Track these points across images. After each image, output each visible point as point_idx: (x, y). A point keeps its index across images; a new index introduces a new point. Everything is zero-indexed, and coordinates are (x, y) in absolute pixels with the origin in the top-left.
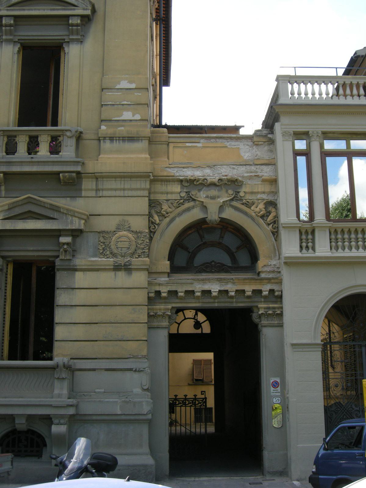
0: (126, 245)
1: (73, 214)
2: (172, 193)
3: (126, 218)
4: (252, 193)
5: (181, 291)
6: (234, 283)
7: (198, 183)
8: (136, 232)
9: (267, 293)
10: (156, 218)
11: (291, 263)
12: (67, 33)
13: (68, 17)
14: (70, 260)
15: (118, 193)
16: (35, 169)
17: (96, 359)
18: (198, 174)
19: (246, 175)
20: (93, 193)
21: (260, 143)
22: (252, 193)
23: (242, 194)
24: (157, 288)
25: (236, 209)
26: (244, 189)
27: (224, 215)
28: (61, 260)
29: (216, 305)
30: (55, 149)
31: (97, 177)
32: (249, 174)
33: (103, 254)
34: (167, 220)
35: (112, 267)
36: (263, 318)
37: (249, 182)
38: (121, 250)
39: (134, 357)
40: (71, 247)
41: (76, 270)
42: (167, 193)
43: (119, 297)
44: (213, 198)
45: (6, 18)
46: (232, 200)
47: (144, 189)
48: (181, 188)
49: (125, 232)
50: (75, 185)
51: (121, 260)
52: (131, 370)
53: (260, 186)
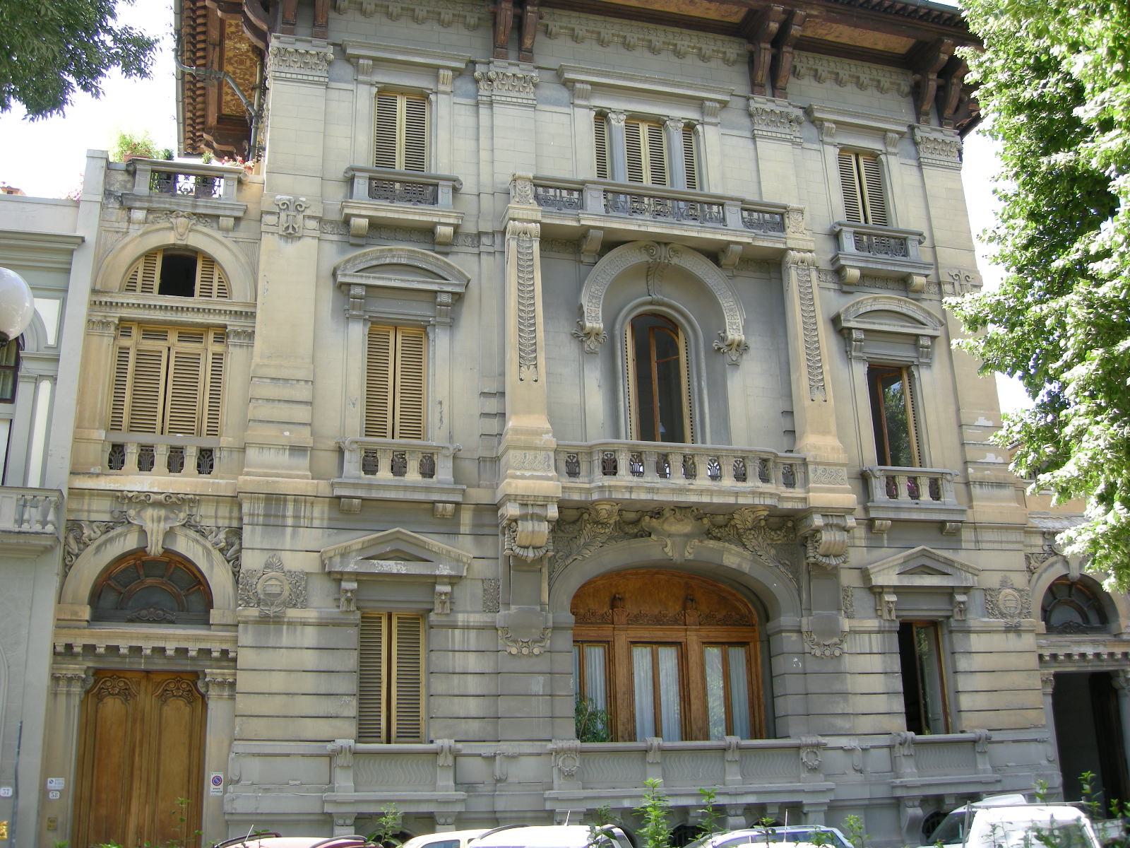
2: (1035, 546)
3: (1008, 574)
5: (1061, 652)
6: (1105, 645)
12: (914, 355)
13: (917, 336)
16: (923, 516)
20: (972, 546)
31: (975, 527)
33: (994, 616)
34: (1036, 576)
35: (1004, 629)
39: (1036, 727)
41: (969, 632)
42: (1031, 546)
43: (1013, 661)
45: (857, 331)
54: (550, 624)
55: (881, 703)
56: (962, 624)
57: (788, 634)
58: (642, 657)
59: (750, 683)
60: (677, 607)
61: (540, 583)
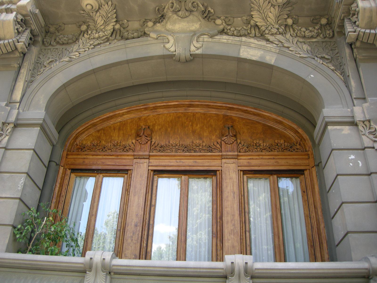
54: (12, 119)
57: (338, 127)
59: (308, 217)
60: (214, 137)
61: (16, 80)
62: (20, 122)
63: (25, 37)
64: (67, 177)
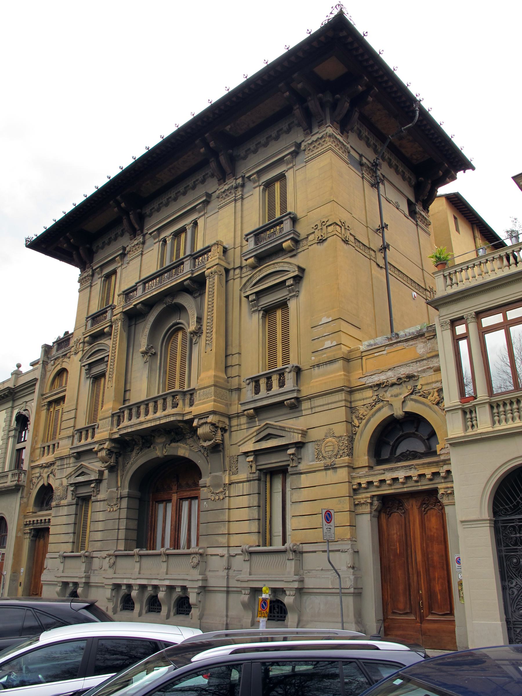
0: (331, 448)
1: (291, 430)
4: (428, 384)
5: (375, 479)
7: (384, 386)
8: (339, 437)
9: (444, 474)
10: (356, 422)
11: (456, 444)
13: (284, 282)
14: (296, 466)
15: (326, 407)
17: (317, 543)
18: (382, 378)
19: (419, 369)
21: (431, 337)
22: (428, 384)
23: (419, 387)
24: (359, 481)
25: (416, 401)
26: (421, 382)
27: (406, 409)
28: (291, 467)
29: (405, 490)
30: (282, 384)
32: (422, 368)
34: (364, 422)
35: (323, 468)
36: (444, 498)
37: (424, 375)
38: (328, 454)
40: (296, 457)
41: (301, 473)
42: (363, 399)
43: (330, 491)
44: (396, 396)
46: (412, 394)
47: (341, 401)
48: (373, 393)
49: (330, 438)
50: (297, 408)
51: (328, 462)
52: (339, 551)
53: (433, 376)
54: (119, 496)
55: (245, 527)
56: (295, 469)
58: (185, 505)
61: (117, 476)
62: (122, 496)
63: (114, 456)
64: (154, 505)
